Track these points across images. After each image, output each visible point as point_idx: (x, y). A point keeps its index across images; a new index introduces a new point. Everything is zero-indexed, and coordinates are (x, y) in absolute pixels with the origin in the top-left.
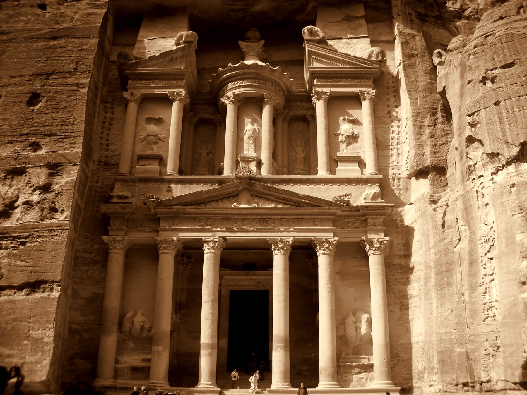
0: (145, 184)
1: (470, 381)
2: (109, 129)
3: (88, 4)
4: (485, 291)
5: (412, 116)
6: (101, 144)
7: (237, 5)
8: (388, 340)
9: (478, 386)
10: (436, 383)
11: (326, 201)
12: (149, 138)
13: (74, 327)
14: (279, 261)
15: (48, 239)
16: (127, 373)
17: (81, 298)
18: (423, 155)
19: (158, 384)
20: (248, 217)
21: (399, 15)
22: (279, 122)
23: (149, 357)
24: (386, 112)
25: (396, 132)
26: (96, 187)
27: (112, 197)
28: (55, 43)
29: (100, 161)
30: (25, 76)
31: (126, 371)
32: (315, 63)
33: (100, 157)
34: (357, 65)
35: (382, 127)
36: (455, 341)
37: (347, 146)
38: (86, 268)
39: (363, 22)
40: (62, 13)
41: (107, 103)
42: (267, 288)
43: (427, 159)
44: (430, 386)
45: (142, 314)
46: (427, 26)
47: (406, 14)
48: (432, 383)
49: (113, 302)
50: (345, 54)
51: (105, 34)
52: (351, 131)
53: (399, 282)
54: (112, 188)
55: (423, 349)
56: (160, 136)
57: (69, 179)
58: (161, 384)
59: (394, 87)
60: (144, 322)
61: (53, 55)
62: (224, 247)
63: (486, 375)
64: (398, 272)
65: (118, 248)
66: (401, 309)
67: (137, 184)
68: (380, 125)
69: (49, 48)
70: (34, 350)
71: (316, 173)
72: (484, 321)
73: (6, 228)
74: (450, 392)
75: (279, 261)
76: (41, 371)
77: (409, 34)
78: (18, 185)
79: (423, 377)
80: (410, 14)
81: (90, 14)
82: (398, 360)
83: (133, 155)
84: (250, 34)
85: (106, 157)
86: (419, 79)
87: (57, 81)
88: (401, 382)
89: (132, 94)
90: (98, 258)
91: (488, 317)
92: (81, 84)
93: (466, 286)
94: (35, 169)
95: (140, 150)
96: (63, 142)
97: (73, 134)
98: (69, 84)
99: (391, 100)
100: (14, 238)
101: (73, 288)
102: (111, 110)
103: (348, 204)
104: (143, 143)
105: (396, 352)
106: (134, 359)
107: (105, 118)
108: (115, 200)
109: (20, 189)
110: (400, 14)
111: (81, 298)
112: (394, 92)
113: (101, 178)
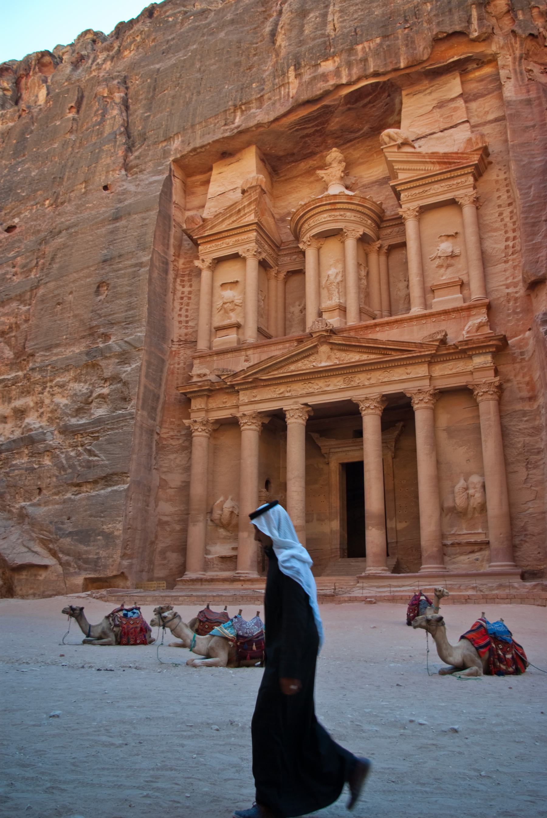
0: (222, 356)
2: (188, 305)
3: (149, 173)
5: (523, 212)
6: (180, 322)
7: (309, 128)
8: (505, 508)
11: (414, 343)
12: (226, 306)
13: (165, 519)
14: (371, 424)
15: (117, 431)
17: (171, 488)
18: (537, 262)
21: (508, 78)
23: (234, 545)
24: (497, 215)
26: (178, 369)
27: (191, 377)
28: (118, 224)
29: (180, 341)
30: (92, 266)
31: (216, 562)
32: (399, 174)
33: (180, 336)
34: (450, 163)
35: (492, 237)
37: (446, 271)
38: (175, 455)
39: (461, 103)
40: (124, 190)
41: (183, 276)
43: (542, 266)
45: (232, 500)
47: (521, 74)
49: (198, 490)
50: (433, 153)
51: (170, 201)
52: (450, 250)
53: (523, 433)
54: (191, 366)
56: (237, 301)
57: (133, 366)
59: (506, 179)
60: (233, 507)
61: (116, 237)
62: (312, 414)
64: (521, 421)
65: (200, 430)
66: (527, 468)
67: (215, 358)
68: (490, 234)
69: (112, 232)
70: (107, 546)
71: (409, 309)
73: (81, 425)
75: (371, 424)
76: (112, 566)
77: (522, 100)
78: (91, 380)
81: (151, 183)
82: (526, 535)
83: (211, 327)
84: (329, 159)
85: (186, 335)
86: (535, 160)
87: (120, 265)
89: (203, 261)
90: (187, 444)
92: (142, 263)
94: (104, 361)
95: (218, 321)
96: (127, 328)
97: (137, 318)
98: (132, 266)
99: (503, 197)
100: (88, 434)
101: (161, 479)
102: (189, 283)
103: (443, 342)
104: (221, 312)
105: (522, 525)
106: (221, 549)
107: (183, 293)
108: (195, 379)
109: (93, 384)
110: (512, 76)
111: (171, 488)
112: (507, 186)
113: (182, 358)
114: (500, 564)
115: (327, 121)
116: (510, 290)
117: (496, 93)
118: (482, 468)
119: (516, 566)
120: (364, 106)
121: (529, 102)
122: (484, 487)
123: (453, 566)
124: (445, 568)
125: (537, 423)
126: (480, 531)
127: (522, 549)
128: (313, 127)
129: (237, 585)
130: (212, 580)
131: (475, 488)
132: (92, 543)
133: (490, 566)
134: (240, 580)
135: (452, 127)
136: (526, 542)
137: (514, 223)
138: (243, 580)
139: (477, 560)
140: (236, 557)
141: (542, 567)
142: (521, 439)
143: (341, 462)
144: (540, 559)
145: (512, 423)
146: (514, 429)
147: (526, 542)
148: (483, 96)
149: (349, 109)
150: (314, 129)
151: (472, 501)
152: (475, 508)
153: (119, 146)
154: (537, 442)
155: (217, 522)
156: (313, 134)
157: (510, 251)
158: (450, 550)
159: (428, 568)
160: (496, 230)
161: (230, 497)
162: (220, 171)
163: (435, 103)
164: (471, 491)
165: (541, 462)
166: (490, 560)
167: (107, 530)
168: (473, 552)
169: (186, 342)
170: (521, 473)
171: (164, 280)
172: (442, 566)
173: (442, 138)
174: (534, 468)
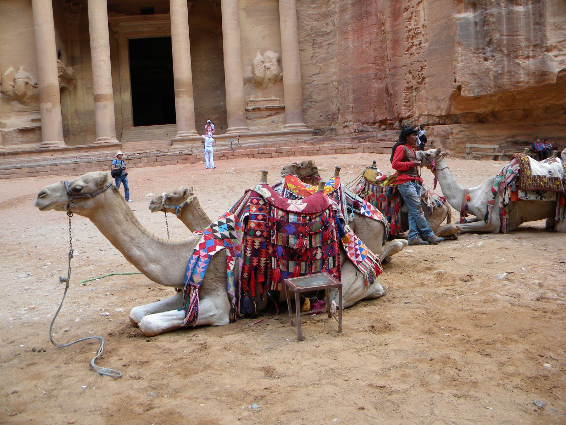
1: (388, 118)
4: (410, 16)
8: (299, 79)
9: (397, 124)
10: (351, 123)
16: (17, 137)
19: (52, 144)
31: (14, 135)
36: (373, 76)
44: (345, 127)
45: (25, 70)
48: (346, 124)
55: (337, 89)
58: (55, 144)
63: (407, 111)
64: (310, 7)
72: (408, 50)
74: (367, 131)
79: (338, 118)
82: (311, 101)
88: (313, 124)
91: (412, 46)
93: (388, 12)
105: (309, 93)
106: (23, 121)
114: (294, 125)
118: (280, 45)
119: (306, 126)
122: (279, 61)
123: (254, 128)
124: (248, 129)
125: (323, 10)
126: (274, 98)
127: (308, 113)
129: (47, 156)
130: (16, 154)
131: (270, 62)
133: (284, 127)
136: (311, 107)
140: (40, 128)
141: (323, 127)
142: (309, 23)
144: (321, 121)
145: (302, 9)
146: (303, 14)
151: (268, 72)
152: (270, 79)
154: (322, 26)
155: (11, 93)
158: (251, 114)
159: (234, 129)
161: (21, 68)
164: (268, 65)
166: (285, 122)
168: (270, 115)
170: (309, 51)
172: (246, 127)
174: (319, 48)
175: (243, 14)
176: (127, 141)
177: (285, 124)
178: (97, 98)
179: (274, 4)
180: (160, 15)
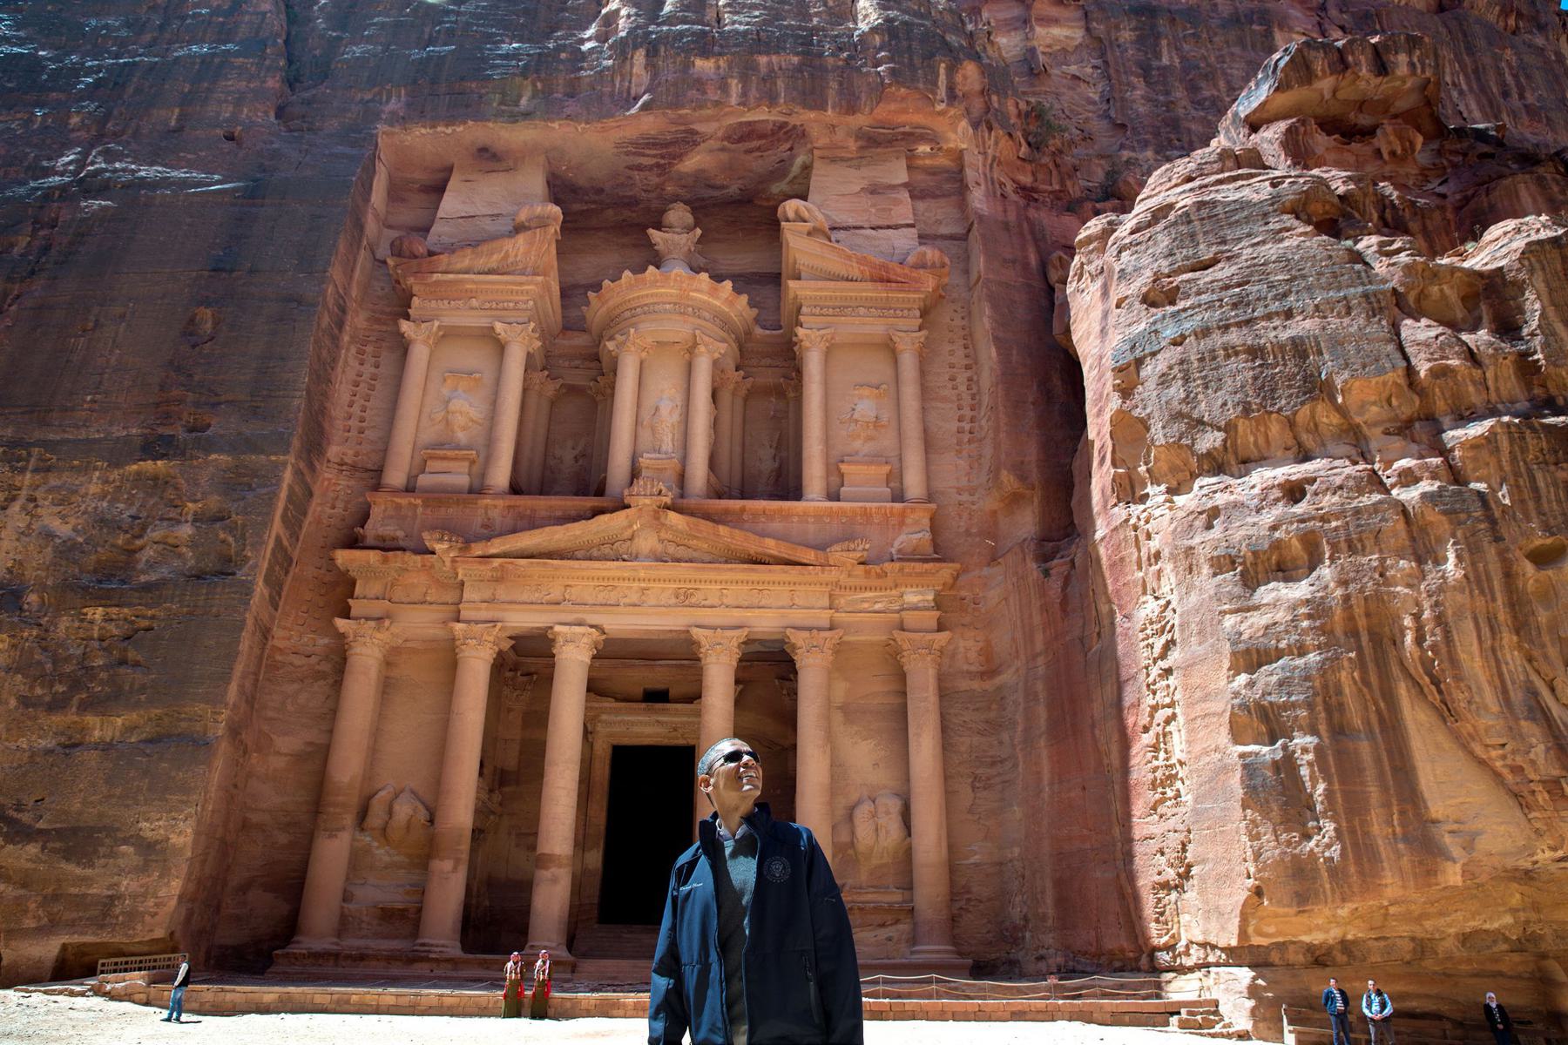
20: (651, 585)
22: (726, 397)
25: (968, 418)
38: (296, 686)
39: (905, 195)
42: (692, 742)
44: (1041, 958)
46: (1037, 209)
49: (347, 767)
66: (973, 788)
70: (144, 869)
76: (154, 915)
80: (1002, 184)
82: (969, 900)
115: (680, 157)
116: (965, 497)
117: (954, 198)
120: (750, 151)
121: (1006, 226)
128: (654, 156)
132: (102, 861)
133: (912, 953)
134: (428, 960)
135: (889, 227)
136: (967, 911)
137: (973, 397)
138: (437, 960)
139: (890, 939)
141: (993, 956)
143: (615, 742)
147: (967, 911)
148: (935, 197)
149: (723, 149)
150: (654, 161)
153: (268, 69)
156: (650, 168)
157: (966, 437)
160: (944, 399)
162: (470, 177)
163: (864, 184)
165: (998, 780)
167: (149, 834)
168: (883, 925)
169: (354, 467)
171: (335, 340)
173: (874, 238)
175: (838, 717)
176: (585, 956)
177: (914, 944)
178: (543, 861)
179: (898, 700)
180: (679, 706)
